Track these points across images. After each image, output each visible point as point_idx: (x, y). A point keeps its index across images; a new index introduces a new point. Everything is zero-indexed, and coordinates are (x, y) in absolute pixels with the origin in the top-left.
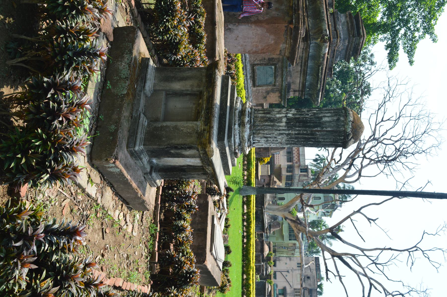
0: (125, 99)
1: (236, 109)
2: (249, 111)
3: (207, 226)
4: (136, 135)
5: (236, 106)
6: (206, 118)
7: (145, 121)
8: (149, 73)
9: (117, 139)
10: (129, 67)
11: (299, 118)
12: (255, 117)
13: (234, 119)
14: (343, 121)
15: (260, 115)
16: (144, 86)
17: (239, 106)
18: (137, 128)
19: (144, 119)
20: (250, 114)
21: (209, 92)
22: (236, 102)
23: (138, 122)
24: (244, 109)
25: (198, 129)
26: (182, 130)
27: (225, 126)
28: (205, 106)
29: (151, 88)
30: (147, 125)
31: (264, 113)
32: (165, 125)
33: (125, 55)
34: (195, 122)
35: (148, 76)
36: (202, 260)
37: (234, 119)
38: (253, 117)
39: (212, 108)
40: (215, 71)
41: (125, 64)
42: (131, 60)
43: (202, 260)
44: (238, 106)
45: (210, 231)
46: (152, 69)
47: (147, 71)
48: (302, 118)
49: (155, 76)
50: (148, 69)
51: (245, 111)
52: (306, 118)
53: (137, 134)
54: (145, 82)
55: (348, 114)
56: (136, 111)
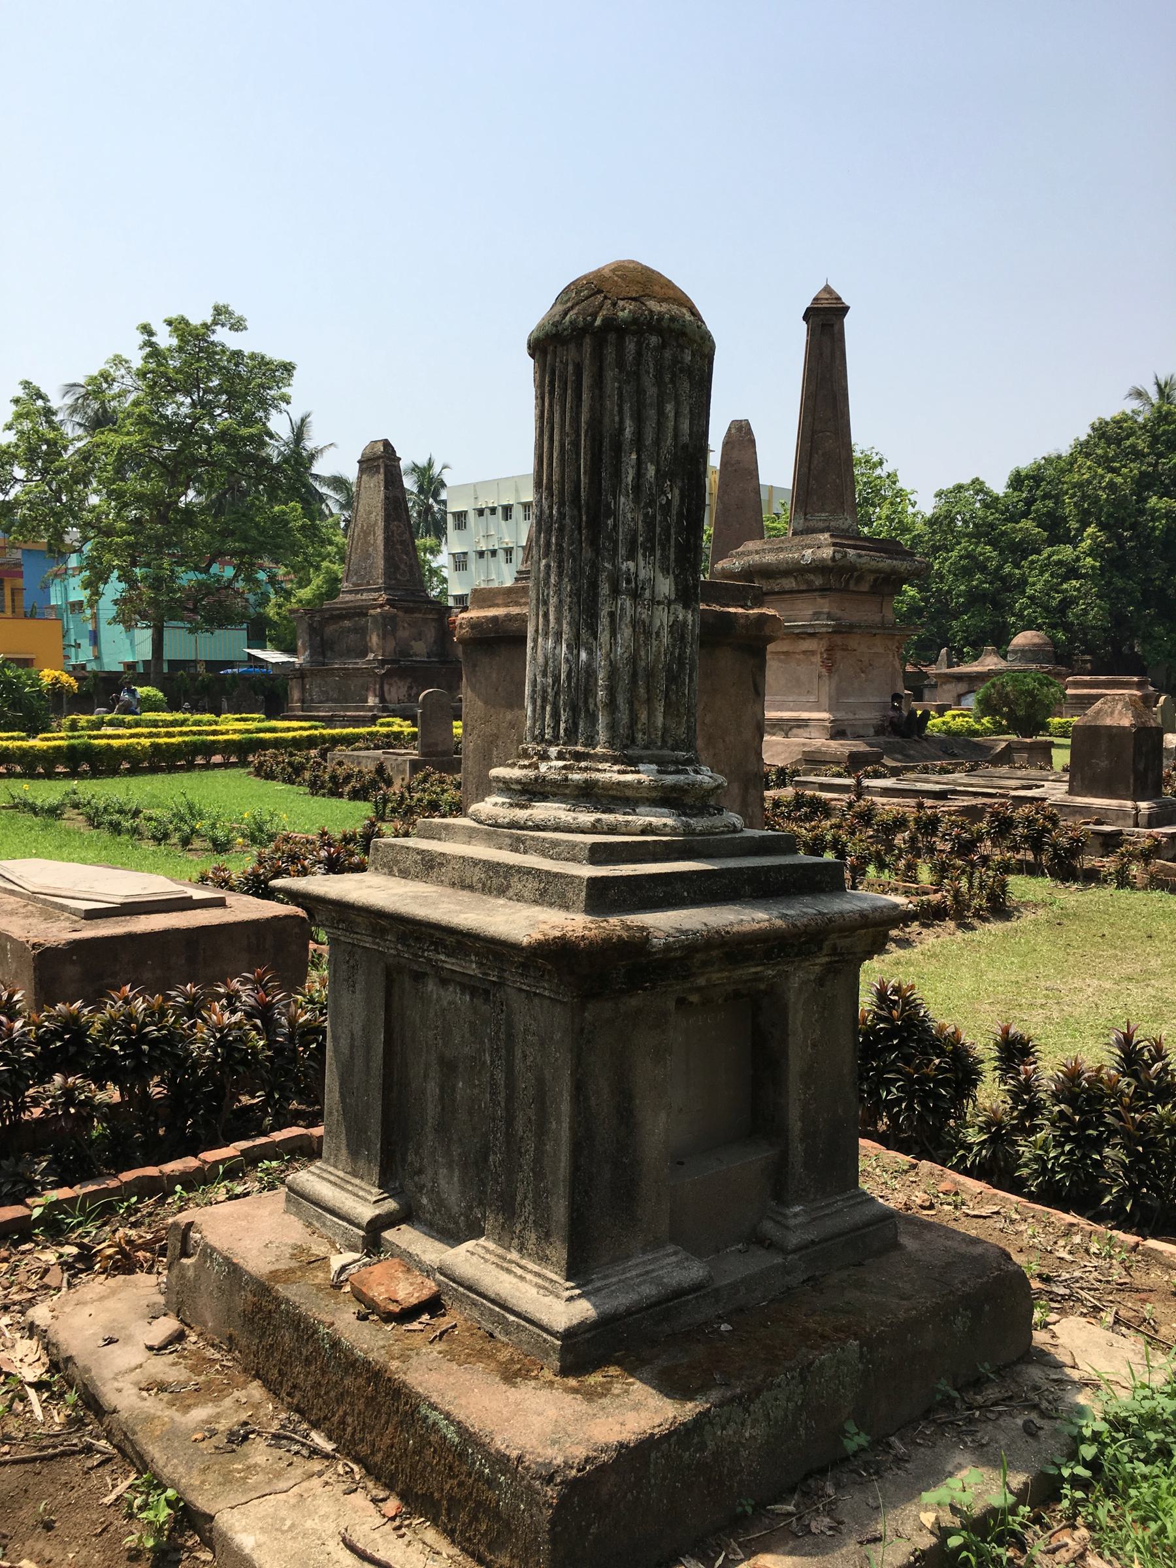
0: (873, 1329)
1: (689, 831)
2: (659, 772)
3: (177, 931)
4: (859, 1229)
5: (674, 831)
6: (796, 955)
7: (796, 1215)
8: (633, 1296)
9: (987, 1282)
10: (758, 1391)
11: (677, 543)
12: (664, 742)
13: (722, 833)
14: (693, 355)
15: (660, 720)
16: (696, 1288)
17: (663, 819)
18: (839, 1235)
19: (796, 1226)
20: (663, 765)
21: (705, 964)
22: (643, 832)
23: (819, 1243)
24: (654, 794)
25: (812, 978)
26: (814, 1045)
27: (779, 868)
28: (753, 970)
29: (675, 1253)
30: (799, 1205)
31: (649, 701)
32: (799, 1124)
33: (711, 1445)
34: (792, 997)
35: (649, 1290)
36: (297, 930)
37: (722, 833)
38: (666, 752)
39: (805, 932)
40: (655, 953)
41: (749, 1422)
42: (732, 1400)
43: (297, 930)
44: (670, 821)
45: (175, 914)
46: (599, 1290)
47: (629, 1312)
48: (678, 533)
49: (614, 1261)
50: (622, 1309)
51: (674, 788)
52: (680, 514)
53: (856, 1228)
54: (679, 1292)
55: (675, 326)
56: (788, 1273)
